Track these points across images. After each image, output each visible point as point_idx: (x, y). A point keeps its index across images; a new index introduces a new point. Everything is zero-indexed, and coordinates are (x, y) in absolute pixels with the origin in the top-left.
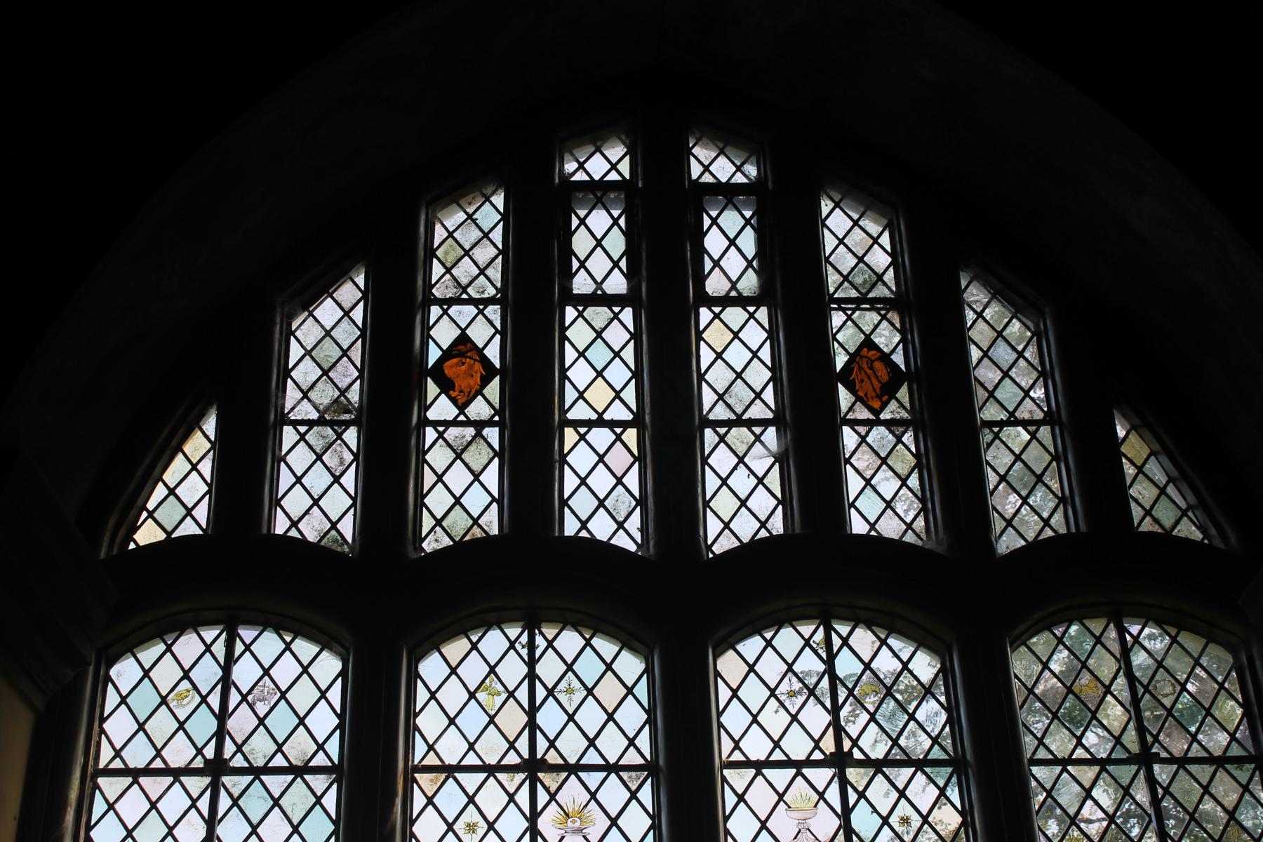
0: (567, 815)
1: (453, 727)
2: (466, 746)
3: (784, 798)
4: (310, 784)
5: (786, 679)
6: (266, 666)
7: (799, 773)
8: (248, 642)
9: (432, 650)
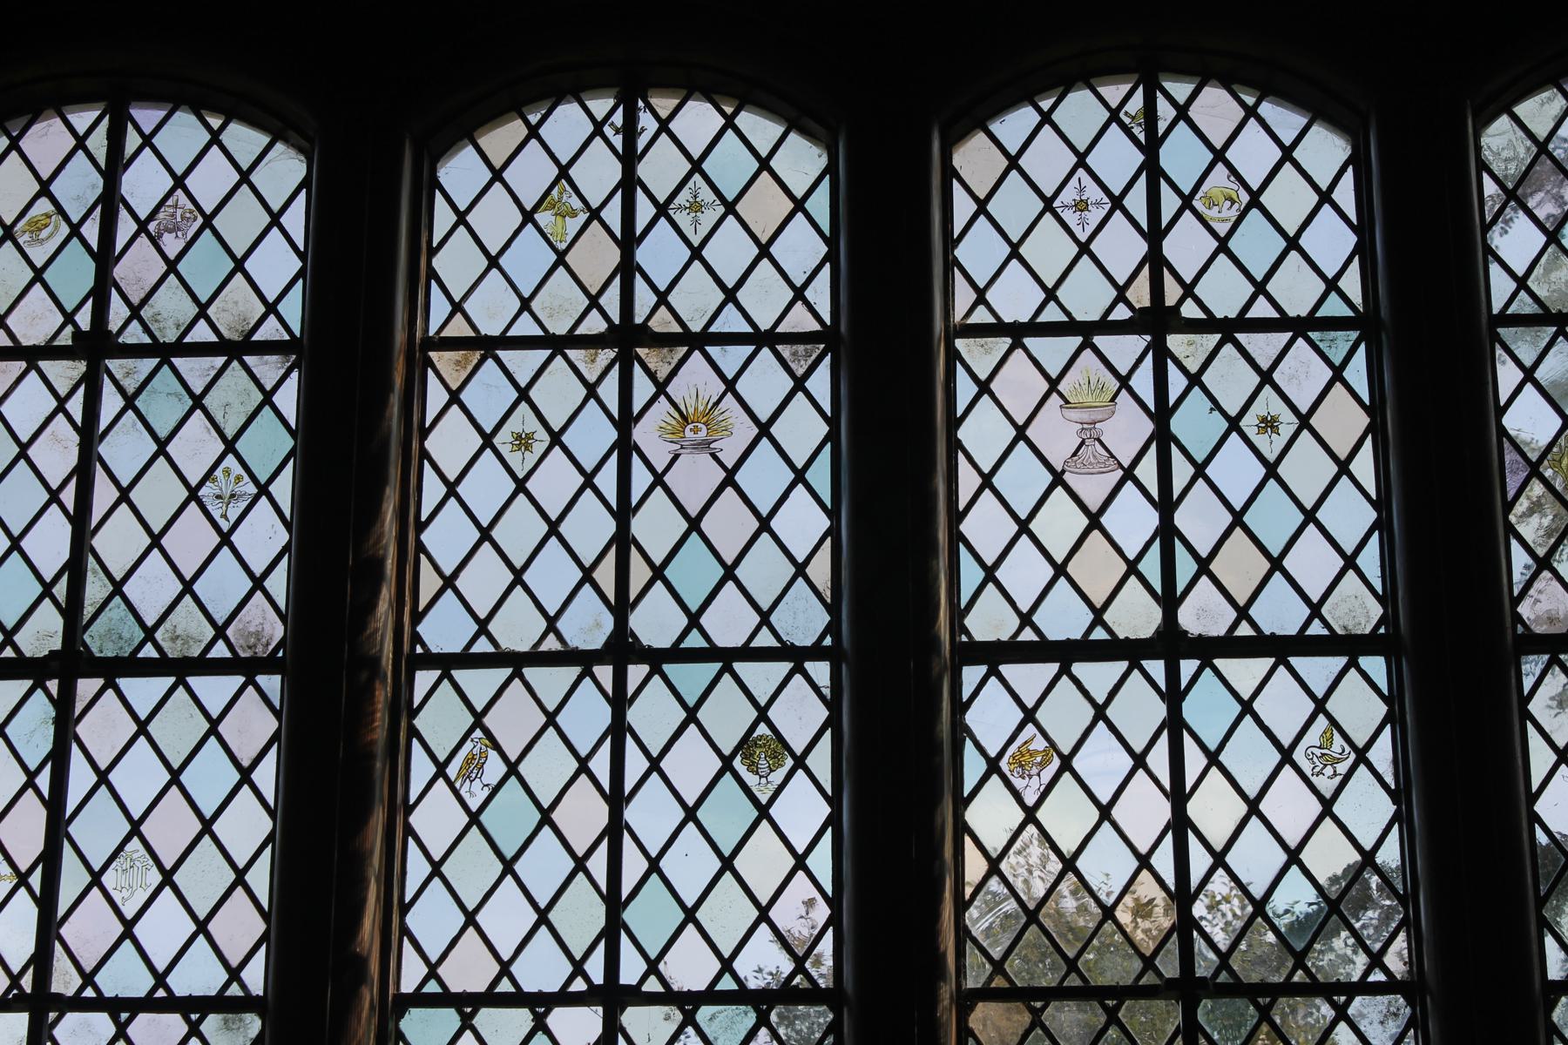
1: (494, 271)
2: (516, 304)
3: (1060, 387)
4: (255, 371)
5: (1074, 182)
6: (179, 171)
7: (1087, 344)
8: (147, 131)
9: (461, 139)
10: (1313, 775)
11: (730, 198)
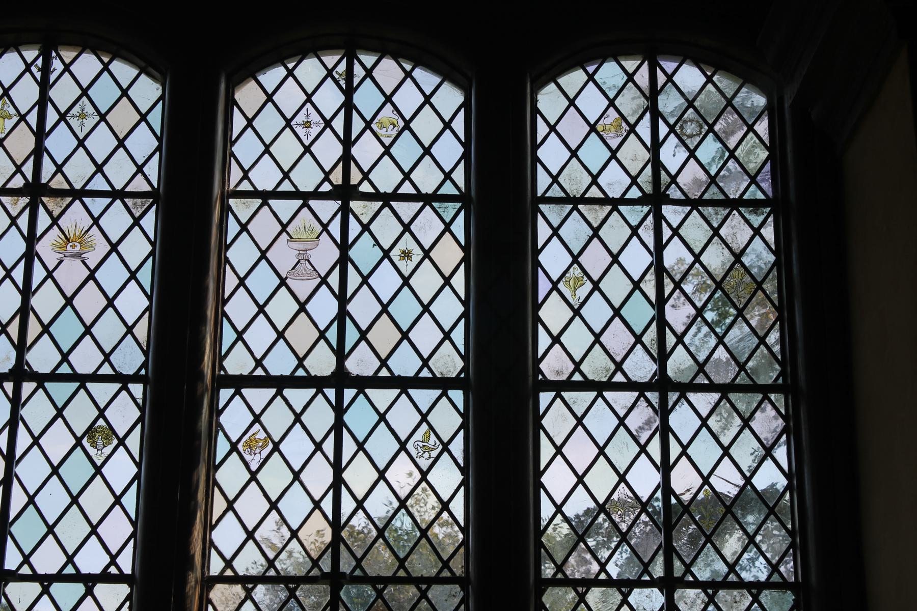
0: (68, 239)
3: (288, 229)
5: (304, 110)
7: (305, 205)
10: (417, 457)
11: (103, 112)
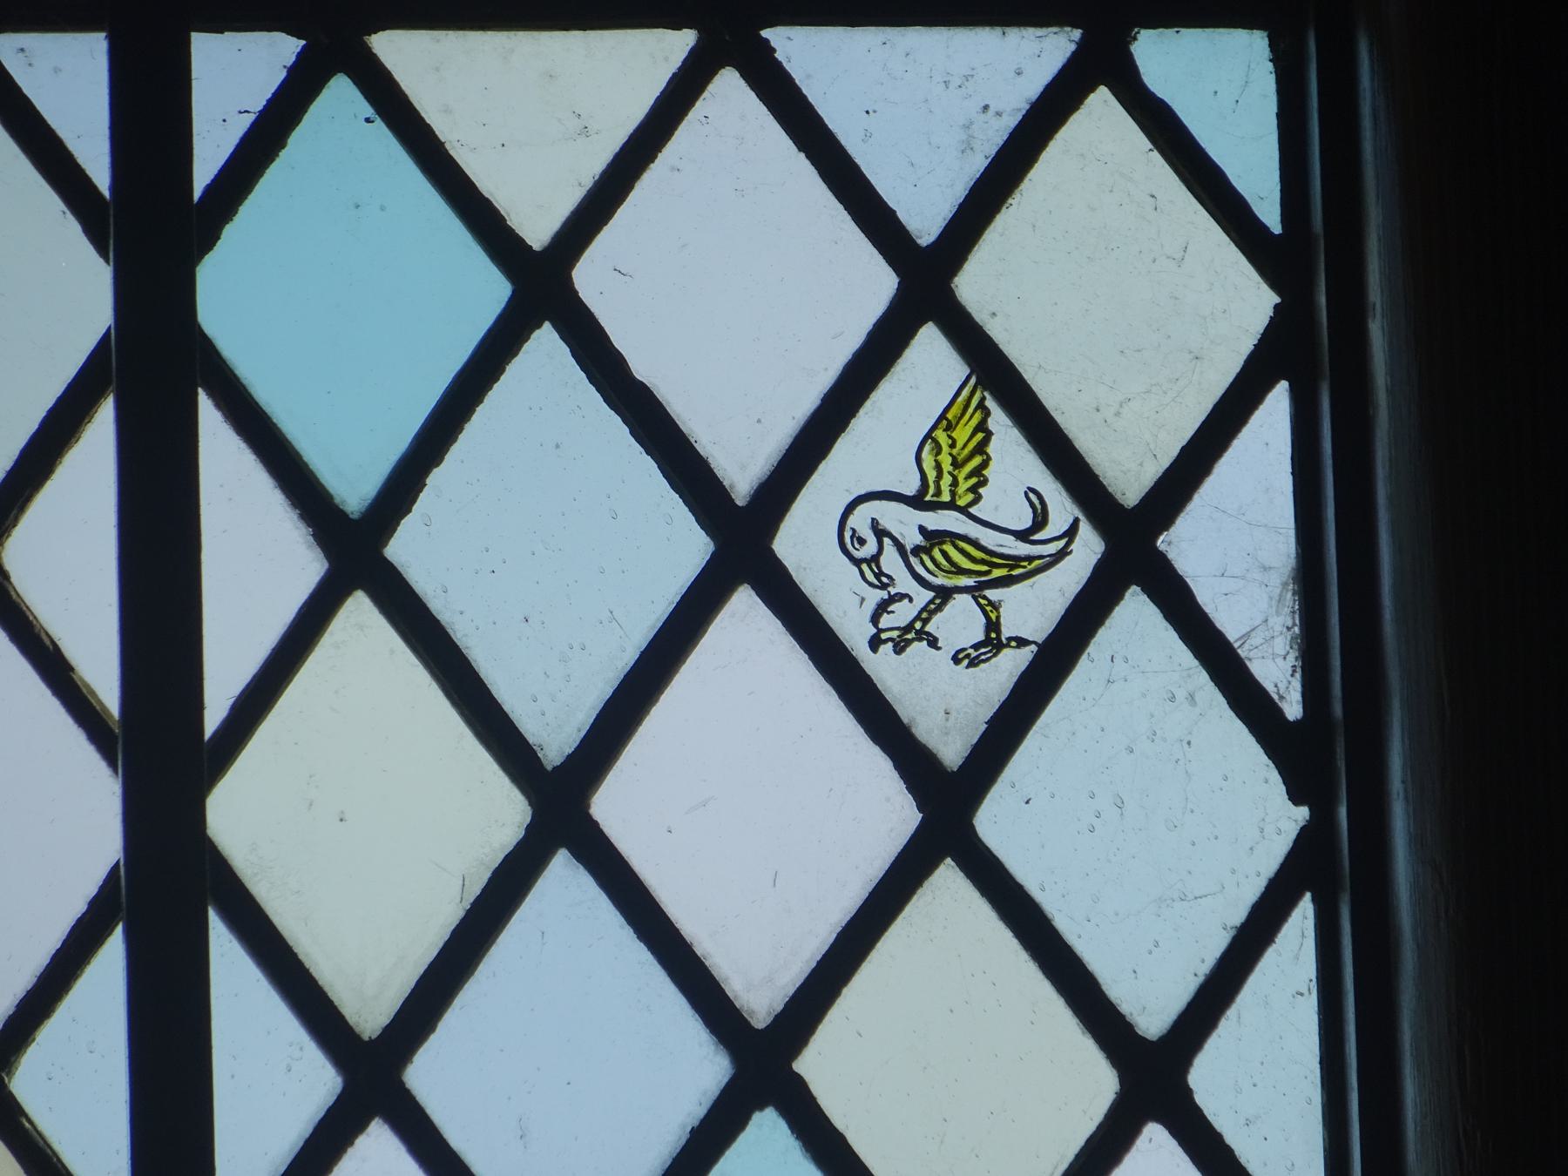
10: (875, 643)
